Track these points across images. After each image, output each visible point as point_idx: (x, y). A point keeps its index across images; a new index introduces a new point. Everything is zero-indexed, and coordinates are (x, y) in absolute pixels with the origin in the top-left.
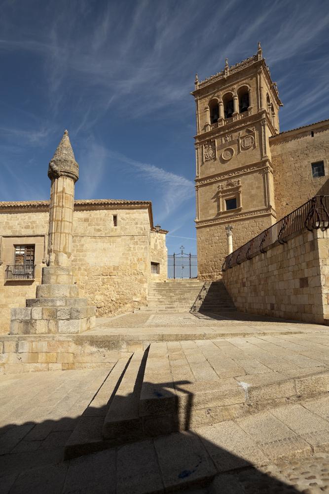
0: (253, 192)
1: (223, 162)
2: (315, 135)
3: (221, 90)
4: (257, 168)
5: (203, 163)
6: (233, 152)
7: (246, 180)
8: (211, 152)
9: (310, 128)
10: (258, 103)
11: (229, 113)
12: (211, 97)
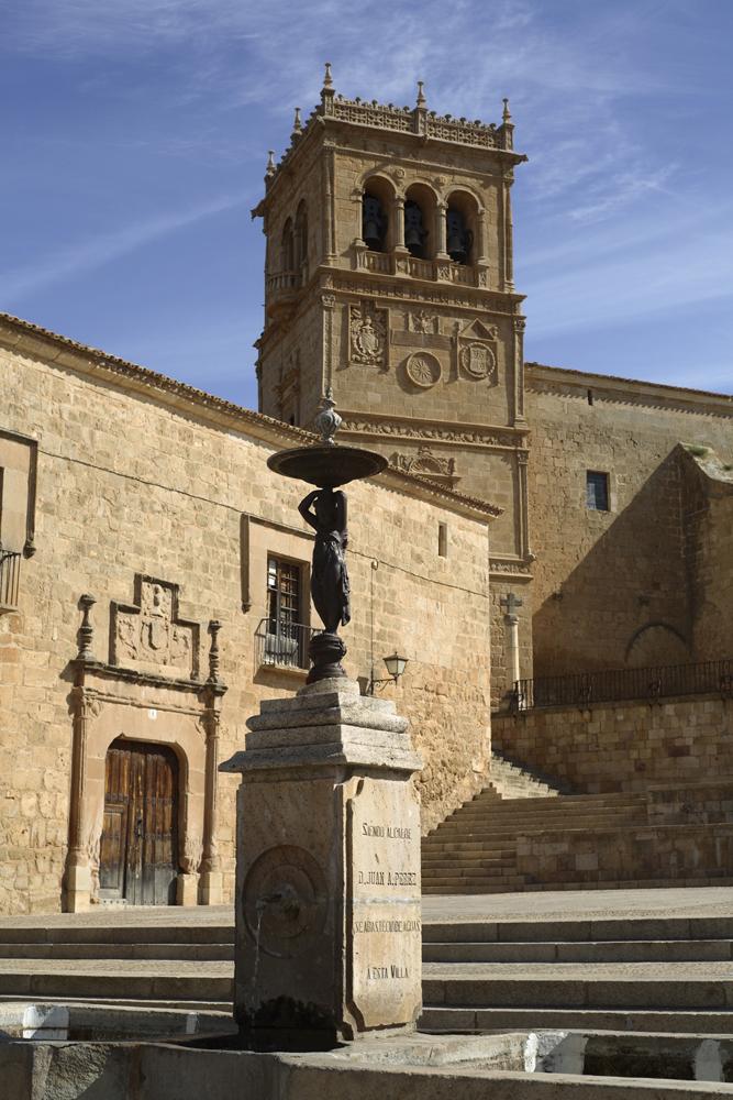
1: (409, 386)
2: (595, 402)
3: (407, 165)
5: (345, 364)
9: (588, 382)
10: (501, 264)
11: (420, 248)
12: (372, 164)
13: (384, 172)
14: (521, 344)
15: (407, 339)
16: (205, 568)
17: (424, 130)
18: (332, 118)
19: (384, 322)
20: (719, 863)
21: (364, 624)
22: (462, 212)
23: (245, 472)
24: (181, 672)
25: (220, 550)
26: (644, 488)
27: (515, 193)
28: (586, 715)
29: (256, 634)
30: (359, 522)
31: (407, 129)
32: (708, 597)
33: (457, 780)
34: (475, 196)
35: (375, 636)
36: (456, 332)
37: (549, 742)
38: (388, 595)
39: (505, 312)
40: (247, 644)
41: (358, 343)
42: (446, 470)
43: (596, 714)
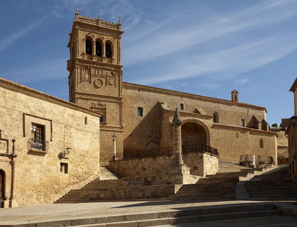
0: (114, 115)
1: (96, 87)
2: (140, 91)
3: (96, 33)
7: (110, 106)
9: (139, 87)
10: (118, 58)
11: (99, 54)
14: (122, 77)
15: (95, 76)
16: (11, 126)
17: (100, 24)
18: (78, 21)
19: (90, 72)
20: (127, 196)
21: (62, 140)
22: (109, 45)
23: (24, 102)
24: (4, 152)
25: (16, 122)
26: (150, 111)
27: (121, 41)
28: (127, 161)
29: (28, 142)
30: (60, 116)
31: (96, 24)
32: (163, 136)
33: (89, 176)
35: (65, 143)
36: (107, 74)
37: (120, 167)
38: (69, 133)
39: (118, 70)
40: (25, 145)
42: (104, 106)
43: (129, 161)
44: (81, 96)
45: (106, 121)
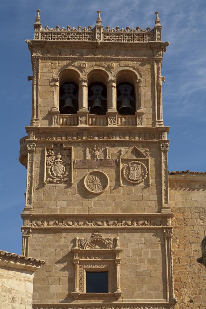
0: (143, 267)
1: (86, 194)
4: (151, 224)
5: (41, 184)
6: (106, 182)
7: (131, 242)
8: (61, 167)
10: (154, 110)
12: (65, 63)
13: (73, 66)
15: (84, 164)
19: (70, 156)
31: (89, 39)
34: (136, 72)
36: (119, 157)
41: (51, 171)
42: (111, 246)
44: (40, 223)
45: (116, 289)
